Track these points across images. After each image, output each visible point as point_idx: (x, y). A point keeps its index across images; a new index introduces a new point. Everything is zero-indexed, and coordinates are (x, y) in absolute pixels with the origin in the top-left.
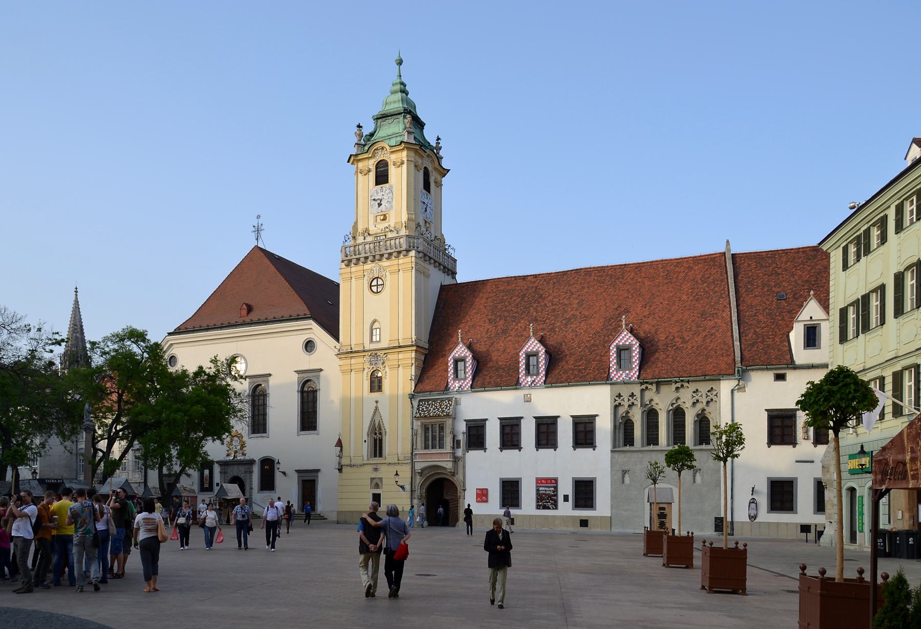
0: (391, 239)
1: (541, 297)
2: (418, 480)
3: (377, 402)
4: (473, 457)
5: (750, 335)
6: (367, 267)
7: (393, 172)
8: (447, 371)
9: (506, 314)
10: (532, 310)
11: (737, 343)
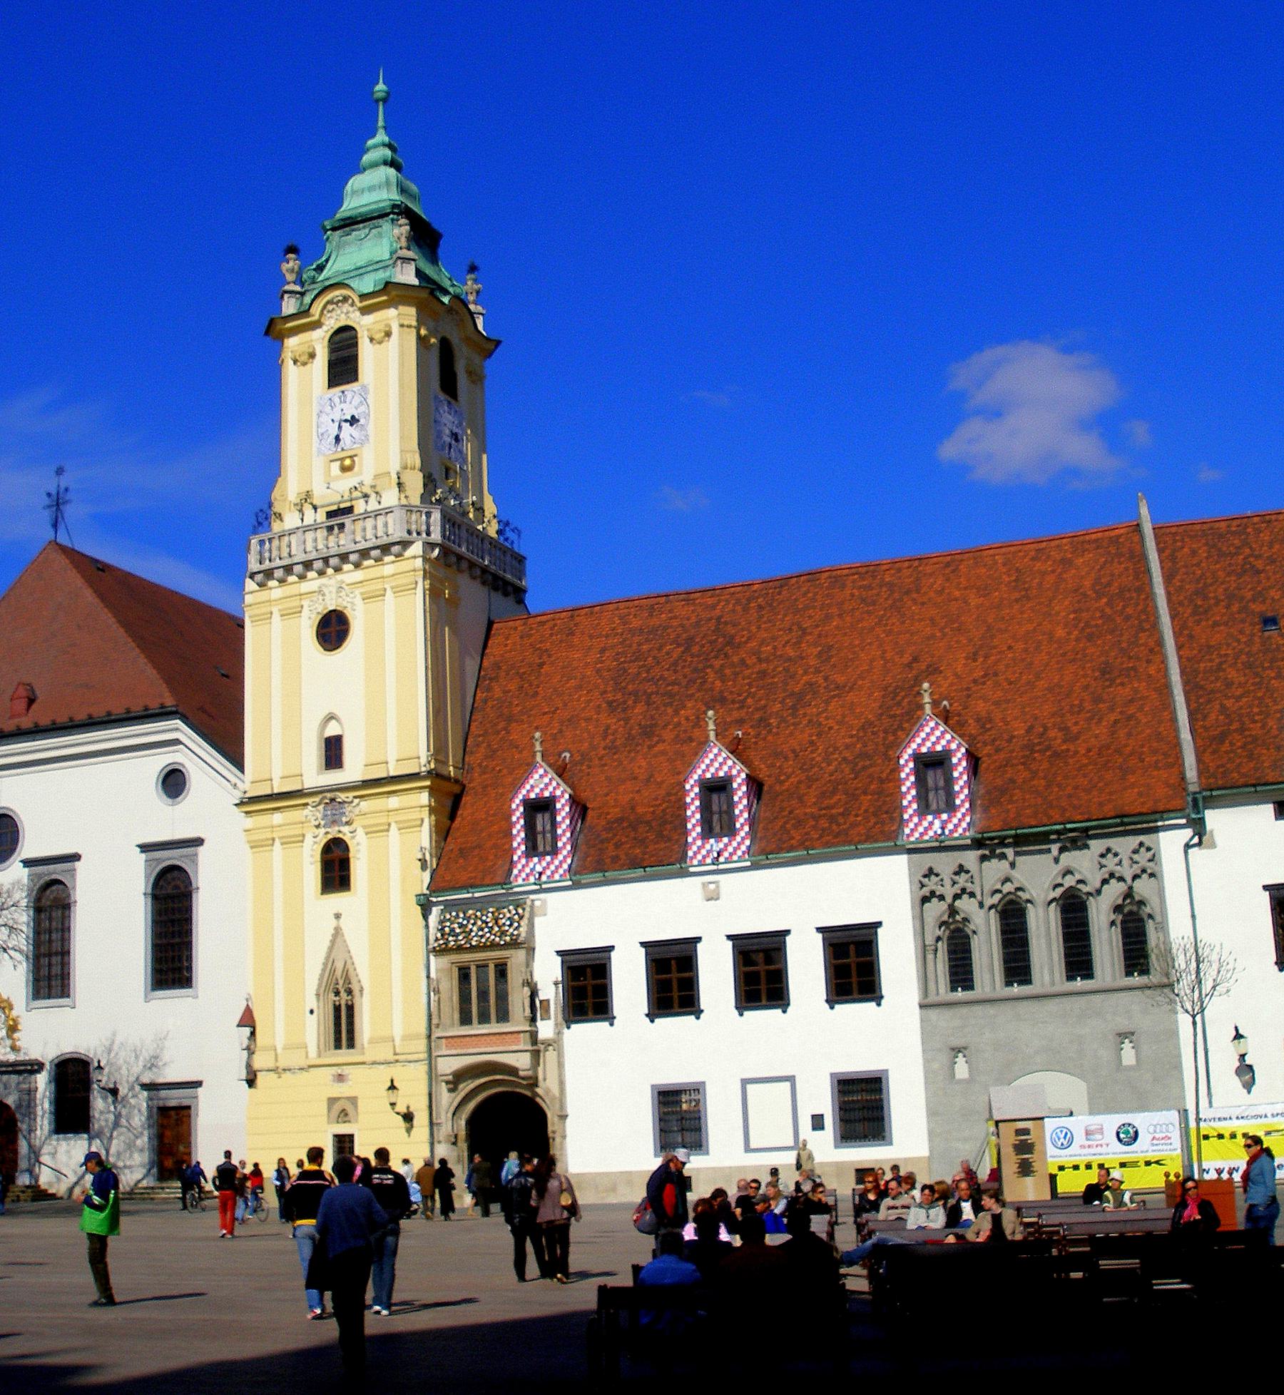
0: (366, 515)
1: (730, 642)
2: (446, 1099)
3: (338, 916)
5: (1213, 716)
6: (305, 587)
7: (366, 353)
8: (511, 837)
9: (650, 688)
10: (711, 676)
11: (1186, 735)
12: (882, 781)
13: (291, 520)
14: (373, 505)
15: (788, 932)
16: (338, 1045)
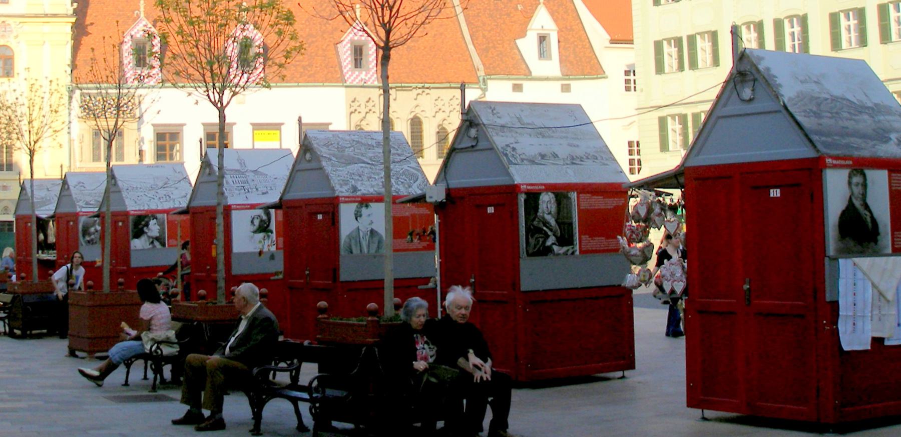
11: (471, 47)
12: (324, 50)
15: (283, 124)
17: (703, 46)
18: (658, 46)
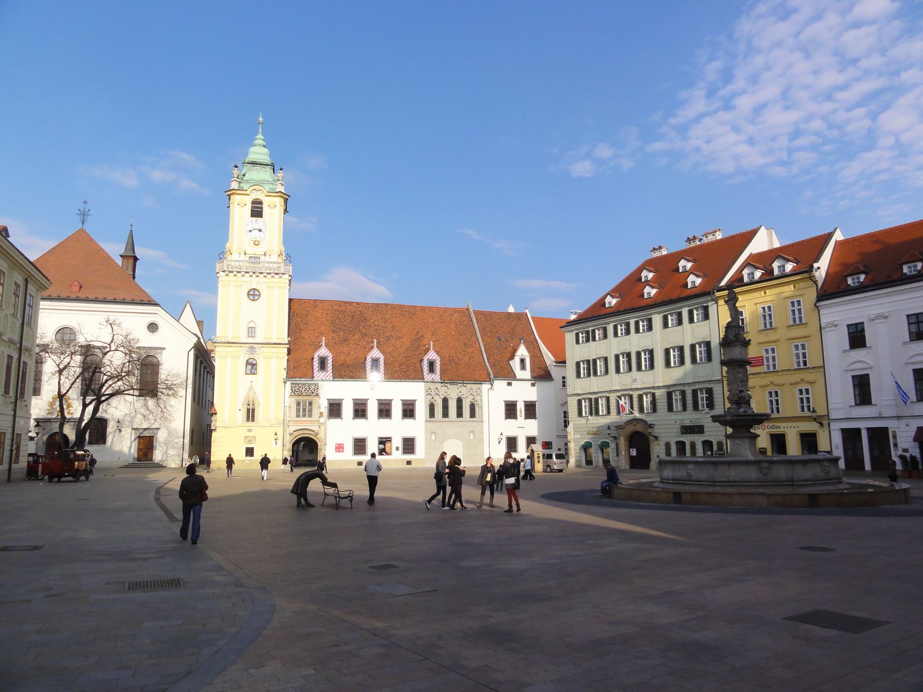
1: (365, 318)
4: (334, 422)
6: (243, 279)
7: (266, 210)
13: (235, 257)
14: (267, 259)
16: (248, 420)
17: (600, 364)
18: (578, 364)
